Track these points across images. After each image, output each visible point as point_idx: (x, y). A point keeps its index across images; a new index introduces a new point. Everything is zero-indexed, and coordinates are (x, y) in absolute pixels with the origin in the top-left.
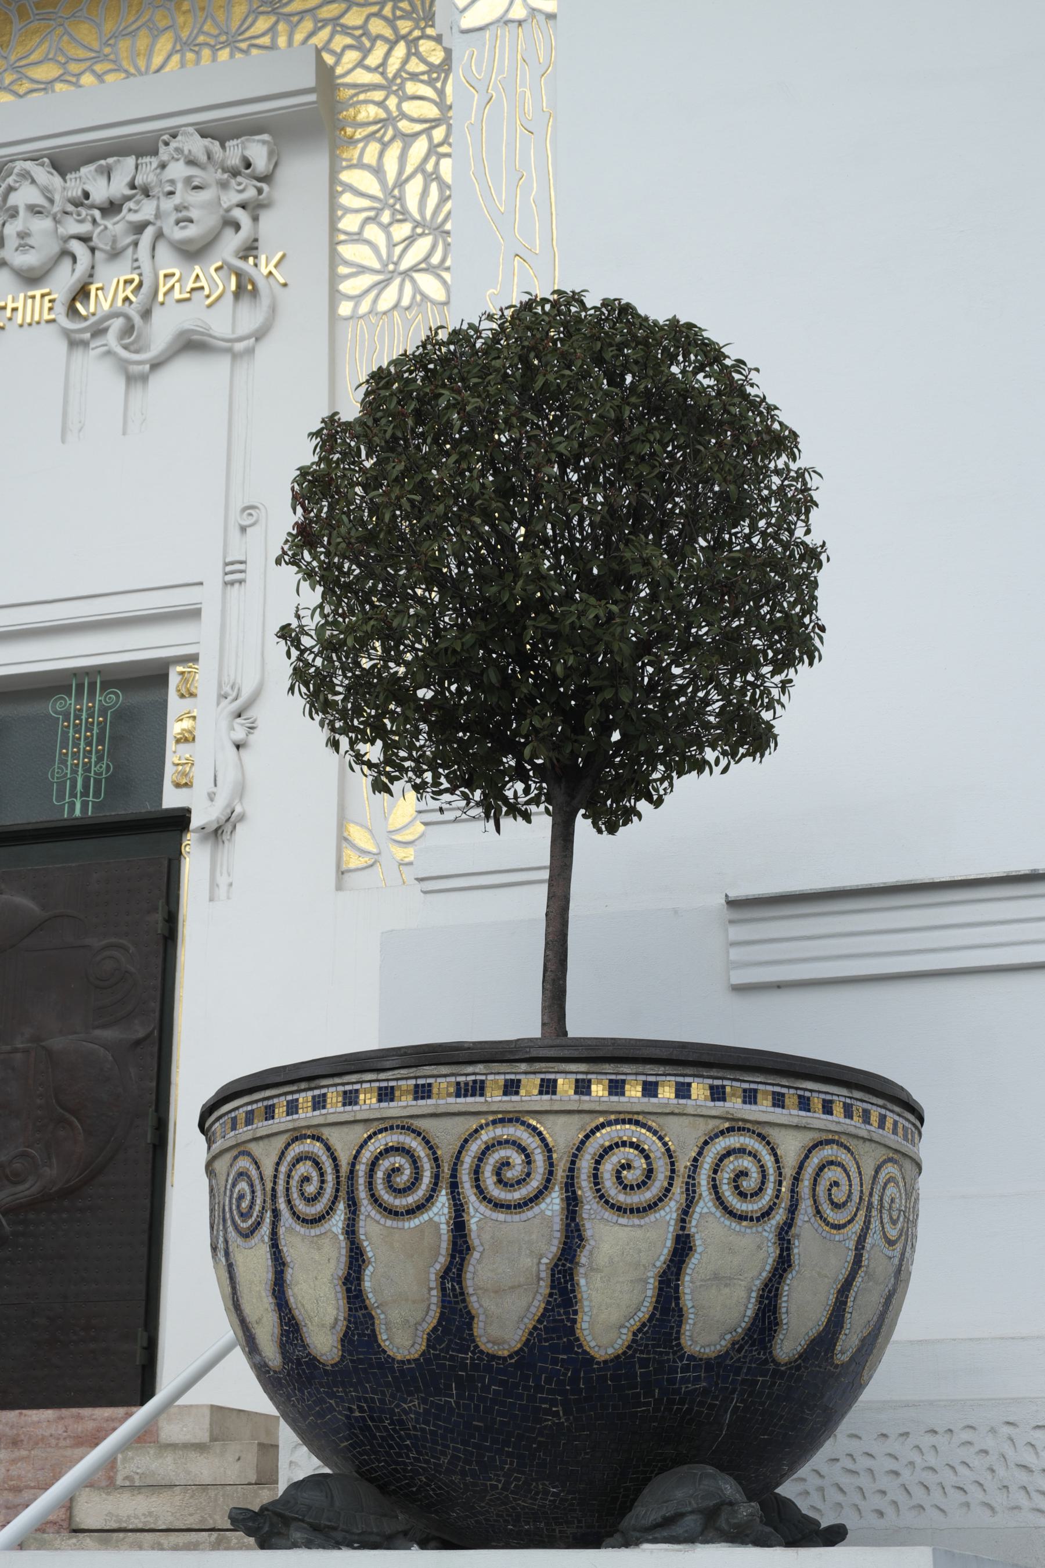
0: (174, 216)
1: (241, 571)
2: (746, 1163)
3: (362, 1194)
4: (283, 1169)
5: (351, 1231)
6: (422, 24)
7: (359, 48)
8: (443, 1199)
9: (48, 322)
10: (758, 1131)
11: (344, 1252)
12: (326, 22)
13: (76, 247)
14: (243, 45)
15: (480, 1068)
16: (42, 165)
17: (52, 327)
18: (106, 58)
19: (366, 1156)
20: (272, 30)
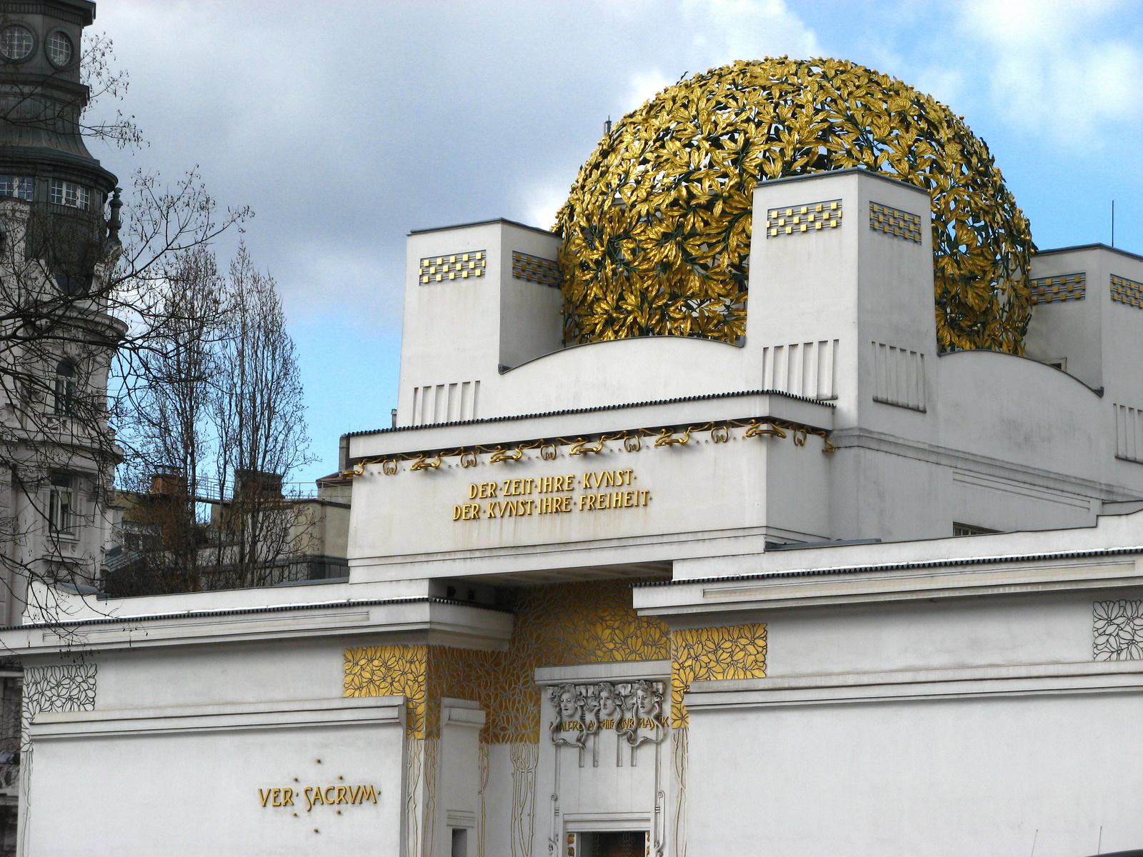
14: (658, 646)
20: (666, 642)
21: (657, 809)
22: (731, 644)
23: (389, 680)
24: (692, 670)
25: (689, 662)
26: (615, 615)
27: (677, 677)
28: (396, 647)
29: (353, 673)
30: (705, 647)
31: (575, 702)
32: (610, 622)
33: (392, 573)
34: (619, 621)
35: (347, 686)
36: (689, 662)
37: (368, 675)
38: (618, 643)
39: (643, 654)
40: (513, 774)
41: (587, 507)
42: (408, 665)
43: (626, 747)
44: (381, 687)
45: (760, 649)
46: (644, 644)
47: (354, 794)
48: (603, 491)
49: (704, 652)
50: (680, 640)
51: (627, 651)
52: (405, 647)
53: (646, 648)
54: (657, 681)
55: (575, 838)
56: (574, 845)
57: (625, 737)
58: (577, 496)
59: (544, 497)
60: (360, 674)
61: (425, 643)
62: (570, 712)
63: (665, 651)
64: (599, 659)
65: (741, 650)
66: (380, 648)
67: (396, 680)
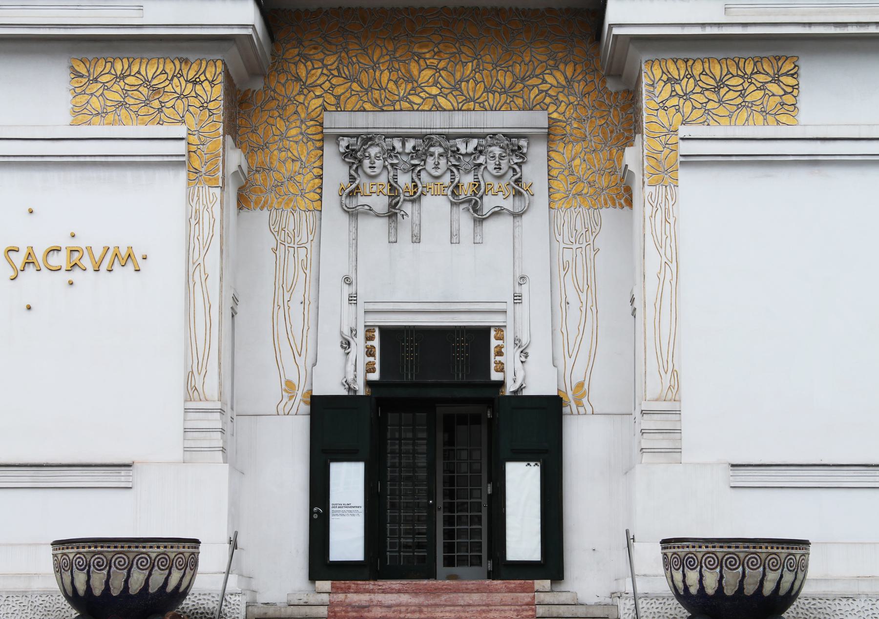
0: (493, 166)
1: (519, 299)
2: (792, 561)
3: (724, 565)
4: (704, 558)
5: (721, 571)
6: (579, 99)
7: (556, 105)
8: (741, 567)
9: (442, 195)
10: (793, 554)
11: (719, 575)
12: (543, 91)
13: (455, 170)
15: (748, 543)
16: (443, 137)
17: (445, 197)
18: (457, 89)
19: (725, 558)
21: (517, 299)
23: (156, 104)
24: (678, 111)
26: (440, 52)
28: (168, 61)
31: (385, 159)
35: (77, 109)
36: (674, 101)
37: (114, 96)
38: (445, 88)
39: (486, 103)
40: (275, 251)
42: (190, 86)
43: (465, 220)
45: (789, 90)
47: (97, 259)
49: (698, 89)
50: (658, 73)
52: (186, 61)
53: (491, 95)
54: (519, 137)
55: (377, 334)
56: (376, 343)
57: (462, 206)
61: (222, 59)
62: (377, 171)
63: (521, 100)
64: (416, 107)
65: (758, 89)
66: (138, 61)
67: (168, 105)
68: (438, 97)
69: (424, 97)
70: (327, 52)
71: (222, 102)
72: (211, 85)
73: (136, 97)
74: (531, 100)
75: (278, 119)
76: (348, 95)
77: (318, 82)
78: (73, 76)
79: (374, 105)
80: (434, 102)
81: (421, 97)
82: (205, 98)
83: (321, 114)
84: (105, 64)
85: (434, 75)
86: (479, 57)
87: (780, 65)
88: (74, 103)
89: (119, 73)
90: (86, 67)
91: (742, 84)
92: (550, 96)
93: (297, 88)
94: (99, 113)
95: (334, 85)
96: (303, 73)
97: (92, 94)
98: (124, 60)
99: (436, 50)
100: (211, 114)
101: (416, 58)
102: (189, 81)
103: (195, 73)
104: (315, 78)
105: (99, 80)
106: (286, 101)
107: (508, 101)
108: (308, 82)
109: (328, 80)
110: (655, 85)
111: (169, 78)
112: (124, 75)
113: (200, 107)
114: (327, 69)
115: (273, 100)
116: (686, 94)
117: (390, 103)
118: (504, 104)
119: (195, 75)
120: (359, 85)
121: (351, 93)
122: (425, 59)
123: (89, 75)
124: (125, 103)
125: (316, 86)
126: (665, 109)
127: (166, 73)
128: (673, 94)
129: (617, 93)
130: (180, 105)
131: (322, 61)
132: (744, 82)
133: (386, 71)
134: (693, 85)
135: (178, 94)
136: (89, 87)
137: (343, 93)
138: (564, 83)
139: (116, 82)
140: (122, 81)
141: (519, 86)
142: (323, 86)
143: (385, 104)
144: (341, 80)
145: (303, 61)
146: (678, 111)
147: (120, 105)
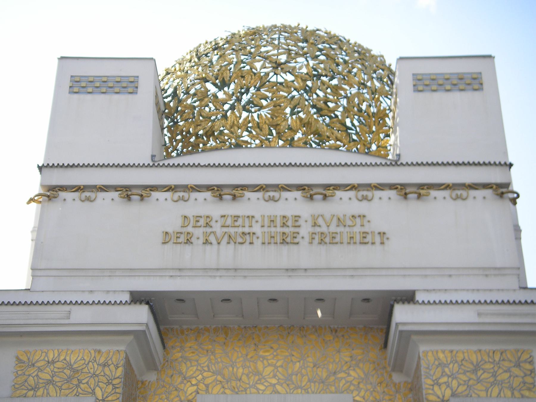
12: (348, 382)
22: (492, 366)
23: (75, 382)
24: (448, 386)
25: (444, 379)
26: (277, 355)
27: (431, 392)
29: (27, 373)
30: (463, 367)
32: (272, 361)
33: (86, 284)
34: (282, 361)
35: (17, 386)
36: (444, 379)
39: (309, 390)
41: (316, 241)
42: (100, 368)
44: (63, 387)
46: (309, 380)
48: (333, 229)
49: (461, 371)
51: (292, 386)
53: (312, 384)
58: (305, 230)
59: (266, 229)
60: (37, 375)
64: (261, 392)
65: (506, 371)
67: (84, 382)
68: (277, 386)
69: (267, 385)
70: (201, 355)
71: (123, 380)
72: (115, 368)
73: (61, 377)
74: (341, 388)
75: (166, 400)
76: (214, 384)
77: (194, 375)
78: (17, 363)
79: (232, 391)
80: (274, 389)
81: (265, 386)
82: (111, 377)
83: (195, 397)
84: (42, 354)
85: (273, 370)
86: (304, 358)
87: (519, 354)
88: (15, 382)
89: (50, 360)
90: (27, 356)
91: (493, 368)
92: (354, 385)
93: (180, 379)
94: (33, 389)
95: (205, 377)
96: (184, 369)
97: (29, 375)
98: (55, 351)
99: (275, 353)
100: (114, 387)
101: (261, 359)
102: (100, 365)
103: (105, 359)
104: (192, 373)
105: (35, 365)
106: (171, 388)
107: (325, 388)
108: (187, 375)
109: (201, 374)
110: (430, 368)
111: (86, 363)
112: (55, 361)
113: (107, 383)
114: (200, 366)
115: (163, 387)
116: (452, 374)
117: (243, 389)
118: (321, 390)
119: (105, 361)
120: (222, 378)
121: (216, 383)
122: (267, 360)
123: (29, 362)
124: (52, 381)
125: (193, 378)
126: (439, 385)
127: (84, 359)
128: (443, 374)
129: (400, 383)
130: (92, 381)
131: (197, 361)
132: (494, 366)
133: (241, 368)
134: (457, 369)
135: (91, 374)
136: (28, 370)
137: (211, 383)
138: (363, 376)
139: (48, 367)
140: (52, 365)
141: (332, 378)
142: (197, 378)
143: (240, 390)
144: (210, 374)
145: (185, 361)
146: (448, 386)
147: (49, 382)
